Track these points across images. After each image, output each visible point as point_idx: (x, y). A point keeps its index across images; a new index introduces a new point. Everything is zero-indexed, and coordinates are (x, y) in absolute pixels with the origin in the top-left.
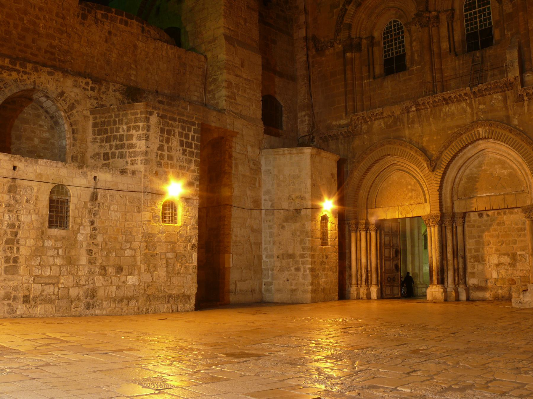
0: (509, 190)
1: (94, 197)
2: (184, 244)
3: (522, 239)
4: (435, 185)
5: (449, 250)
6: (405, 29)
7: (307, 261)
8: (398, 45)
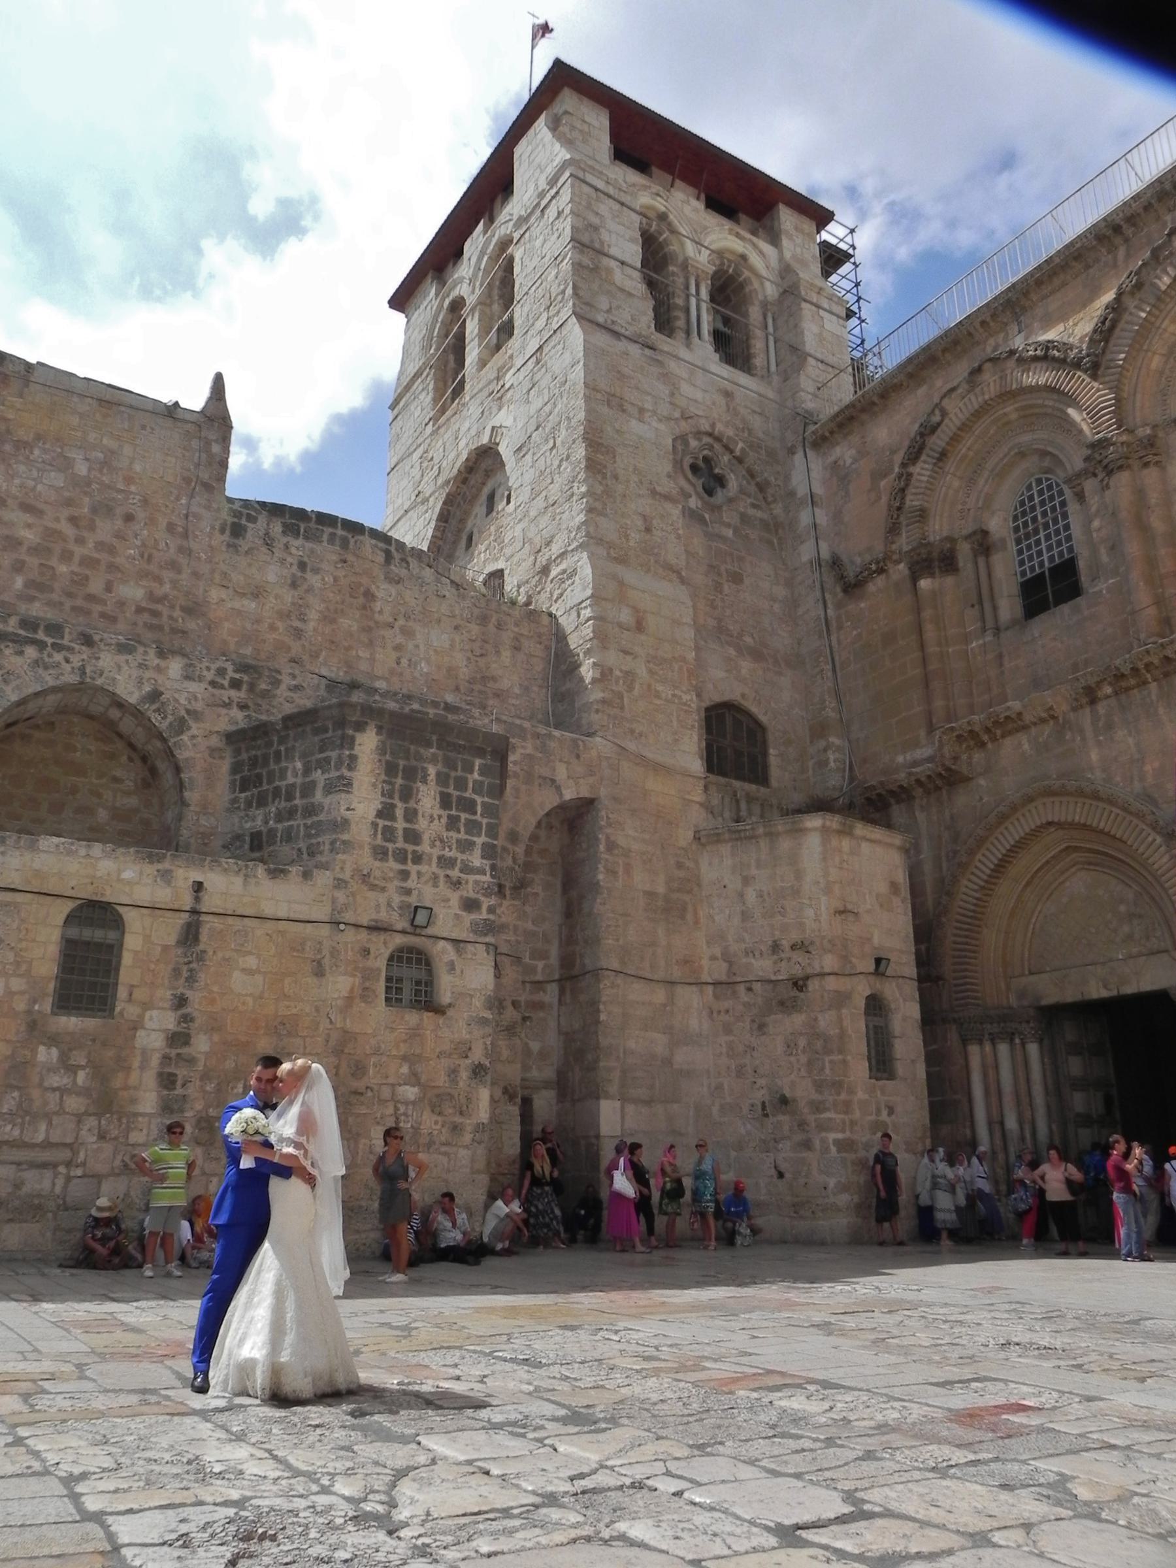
1: (190, 935)
2: (445, 1062)
6: (1068, 494)
7: (830, 1119)
8: (1054, 539)
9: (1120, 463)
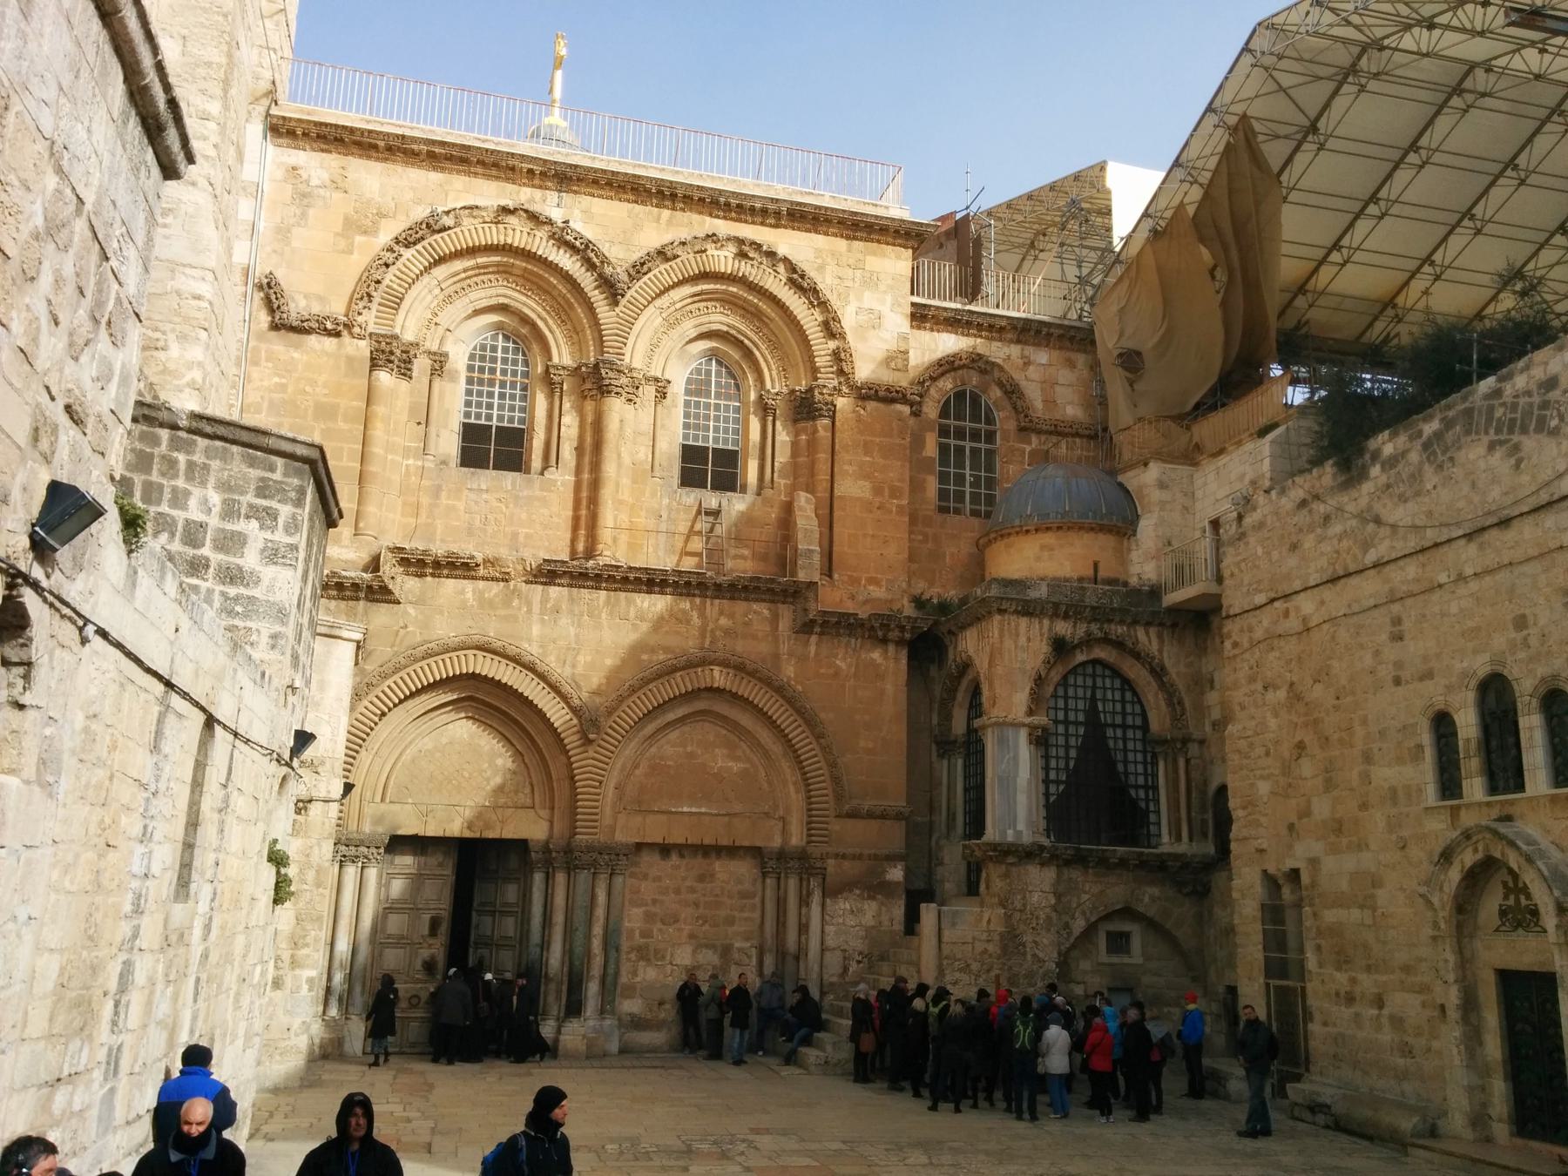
0: (738, 807)
3: (746, 915)
5: (598, 930)
9: (619, 390)
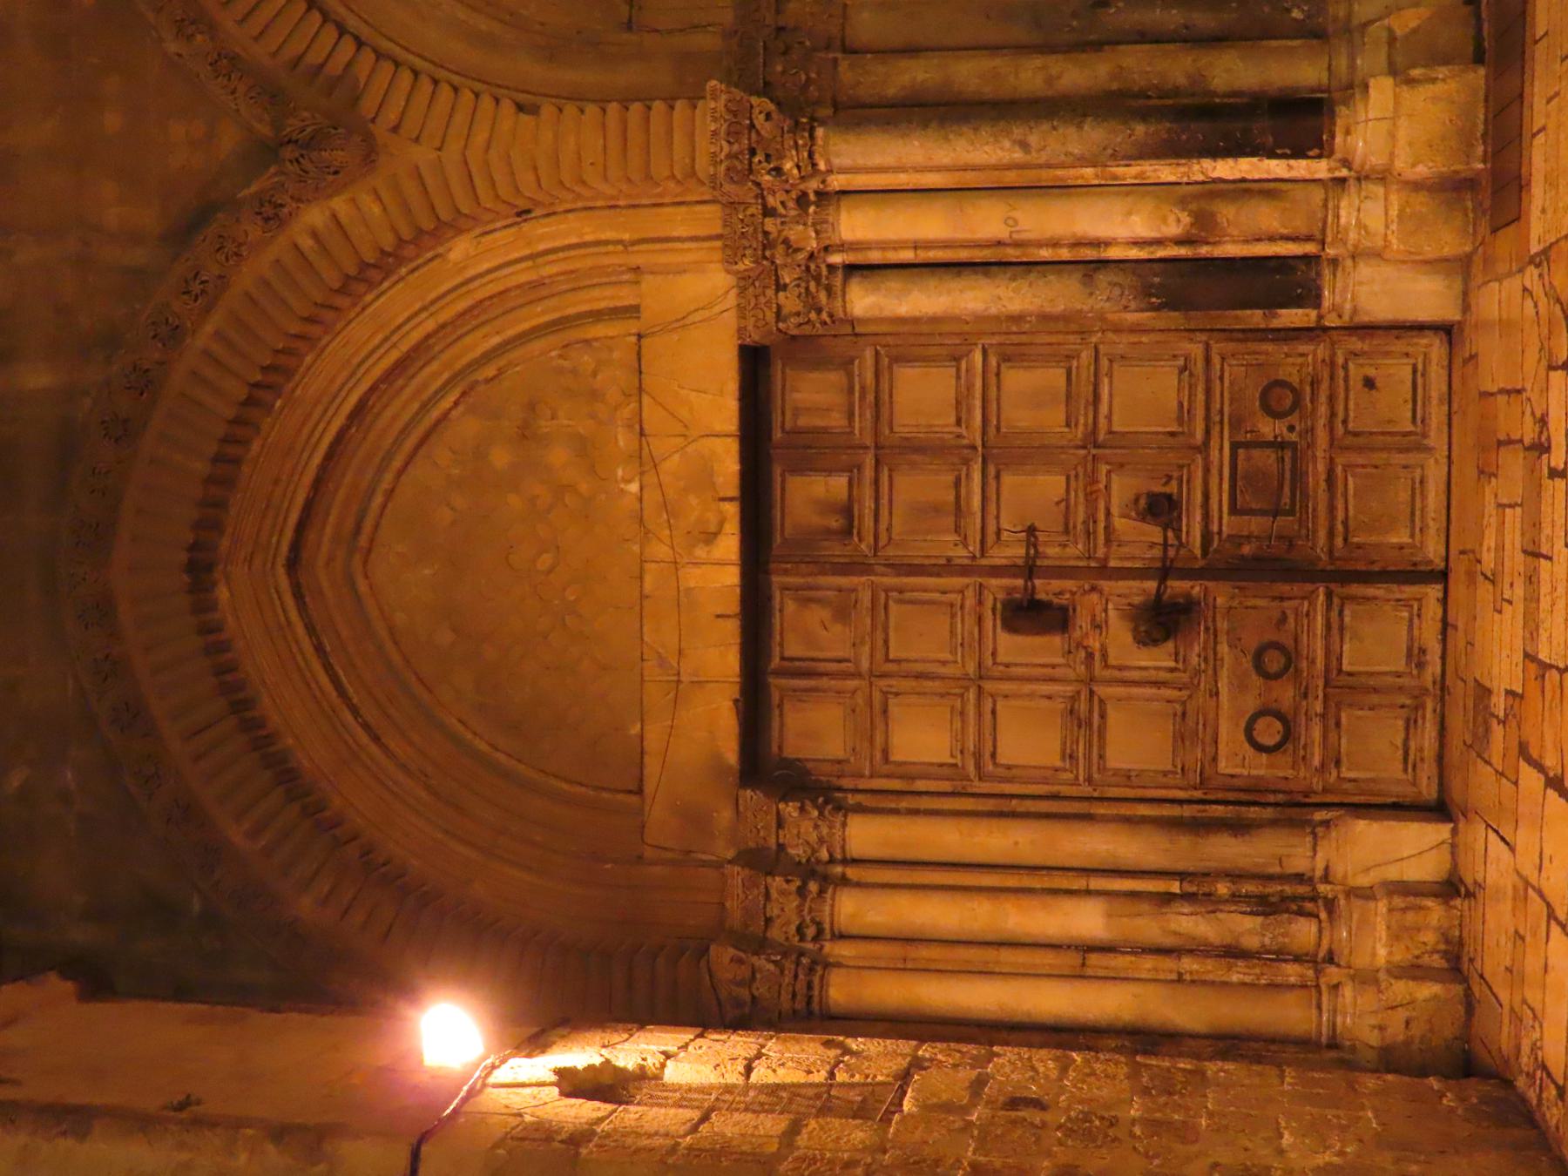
4: (480, 138)
